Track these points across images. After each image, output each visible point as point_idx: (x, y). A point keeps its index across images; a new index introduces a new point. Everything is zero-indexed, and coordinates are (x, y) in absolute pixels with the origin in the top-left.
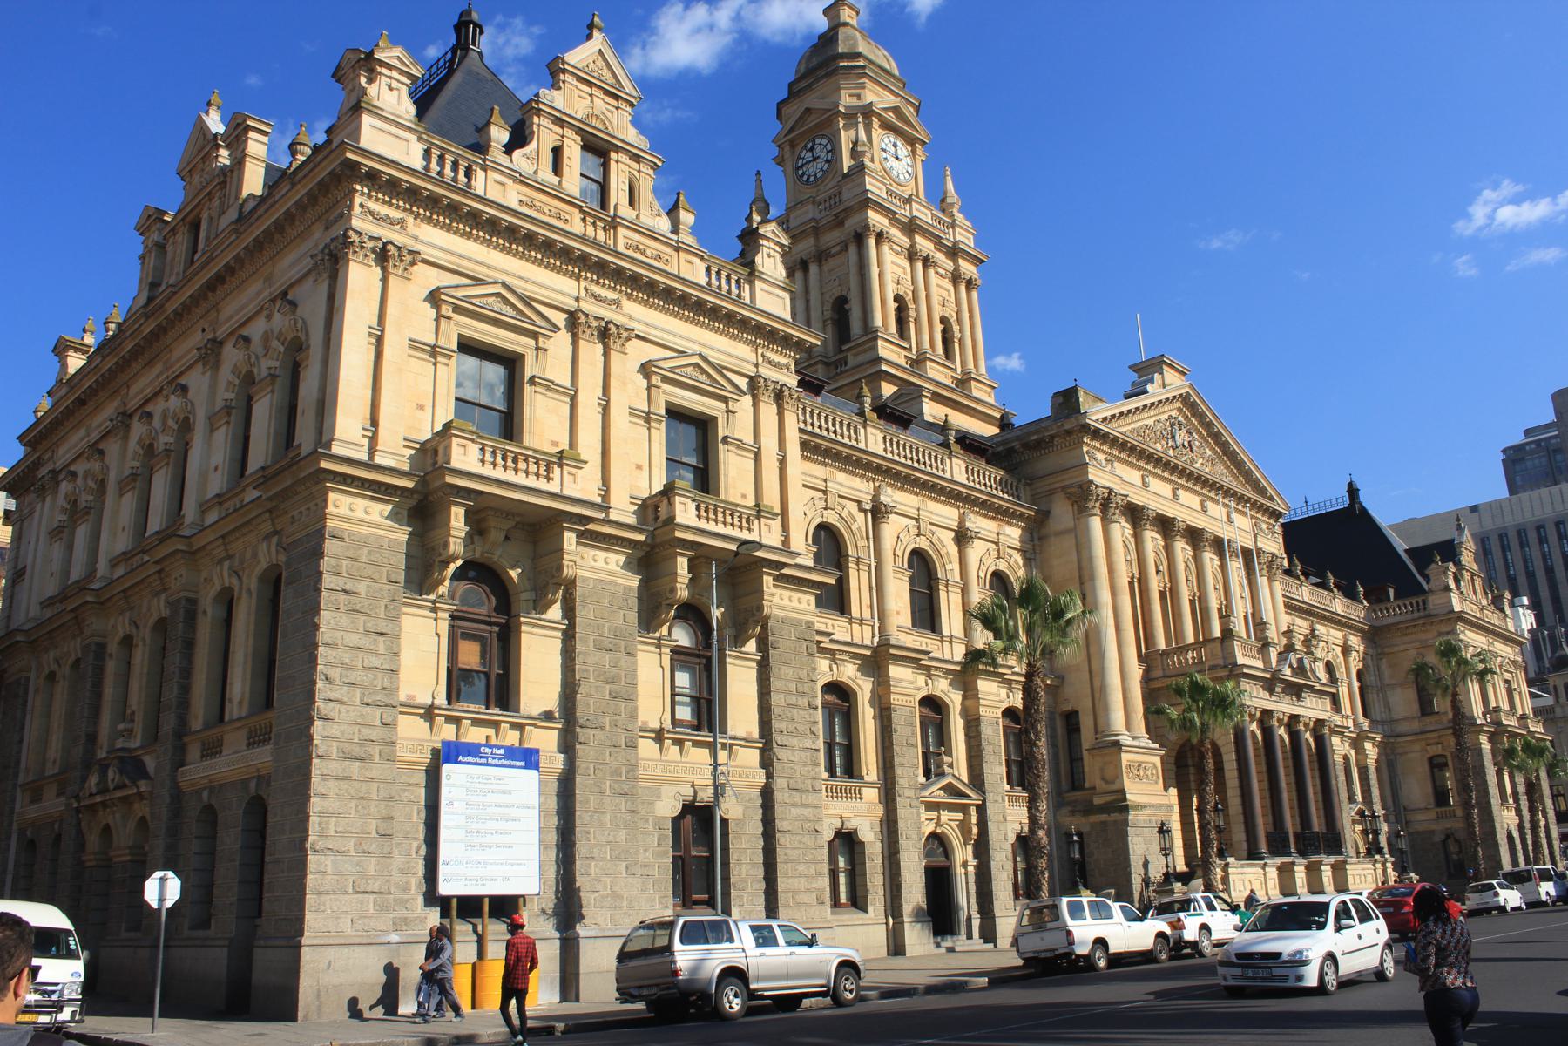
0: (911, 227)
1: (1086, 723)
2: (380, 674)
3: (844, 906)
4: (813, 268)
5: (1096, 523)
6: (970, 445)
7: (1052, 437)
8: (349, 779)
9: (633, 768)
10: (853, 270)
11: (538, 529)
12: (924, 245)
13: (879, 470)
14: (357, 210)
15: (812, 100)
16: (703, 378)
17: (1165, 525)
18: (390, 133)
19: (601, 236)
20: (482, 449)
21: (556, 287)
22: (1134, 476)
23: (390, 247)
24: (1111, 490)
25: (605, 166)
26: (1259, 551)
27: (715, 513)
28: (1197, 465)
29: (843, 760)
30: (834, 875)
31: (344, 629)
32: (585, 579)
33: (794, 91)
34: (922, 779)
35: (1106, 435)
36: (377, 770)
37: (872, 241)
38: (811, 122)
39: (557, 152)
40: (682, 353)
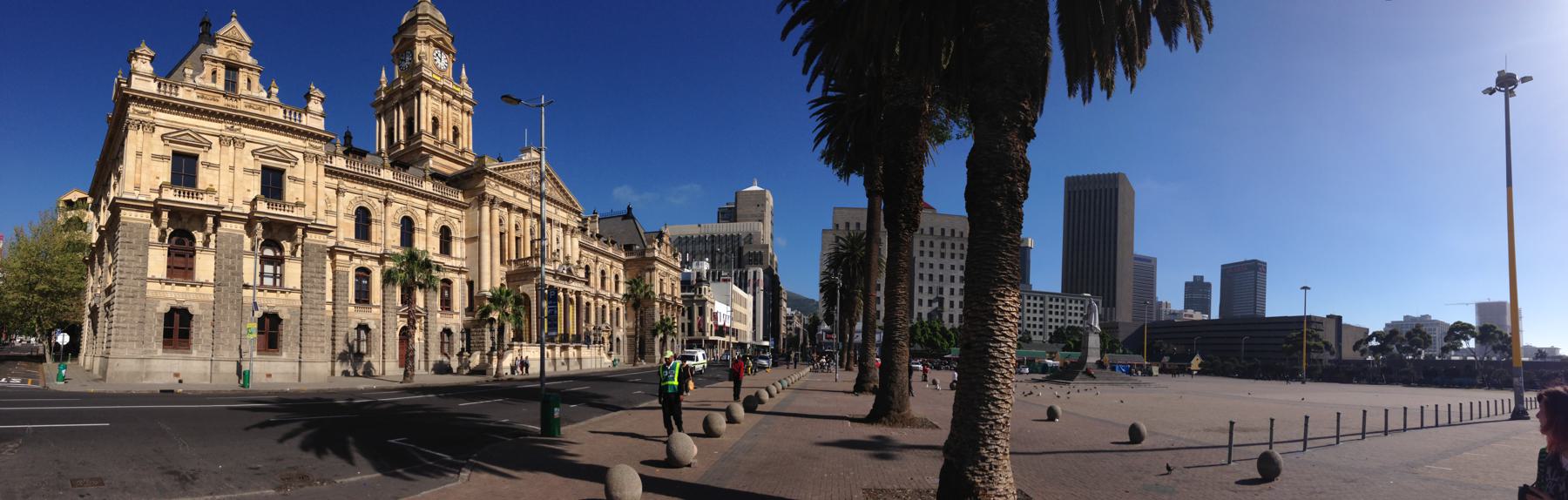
5: (486, 210)
6: (437, 176)
11: (198, 217)
15: (408, 34)
18: (144, 83)
22: (510, 192)
37: (423, 95)
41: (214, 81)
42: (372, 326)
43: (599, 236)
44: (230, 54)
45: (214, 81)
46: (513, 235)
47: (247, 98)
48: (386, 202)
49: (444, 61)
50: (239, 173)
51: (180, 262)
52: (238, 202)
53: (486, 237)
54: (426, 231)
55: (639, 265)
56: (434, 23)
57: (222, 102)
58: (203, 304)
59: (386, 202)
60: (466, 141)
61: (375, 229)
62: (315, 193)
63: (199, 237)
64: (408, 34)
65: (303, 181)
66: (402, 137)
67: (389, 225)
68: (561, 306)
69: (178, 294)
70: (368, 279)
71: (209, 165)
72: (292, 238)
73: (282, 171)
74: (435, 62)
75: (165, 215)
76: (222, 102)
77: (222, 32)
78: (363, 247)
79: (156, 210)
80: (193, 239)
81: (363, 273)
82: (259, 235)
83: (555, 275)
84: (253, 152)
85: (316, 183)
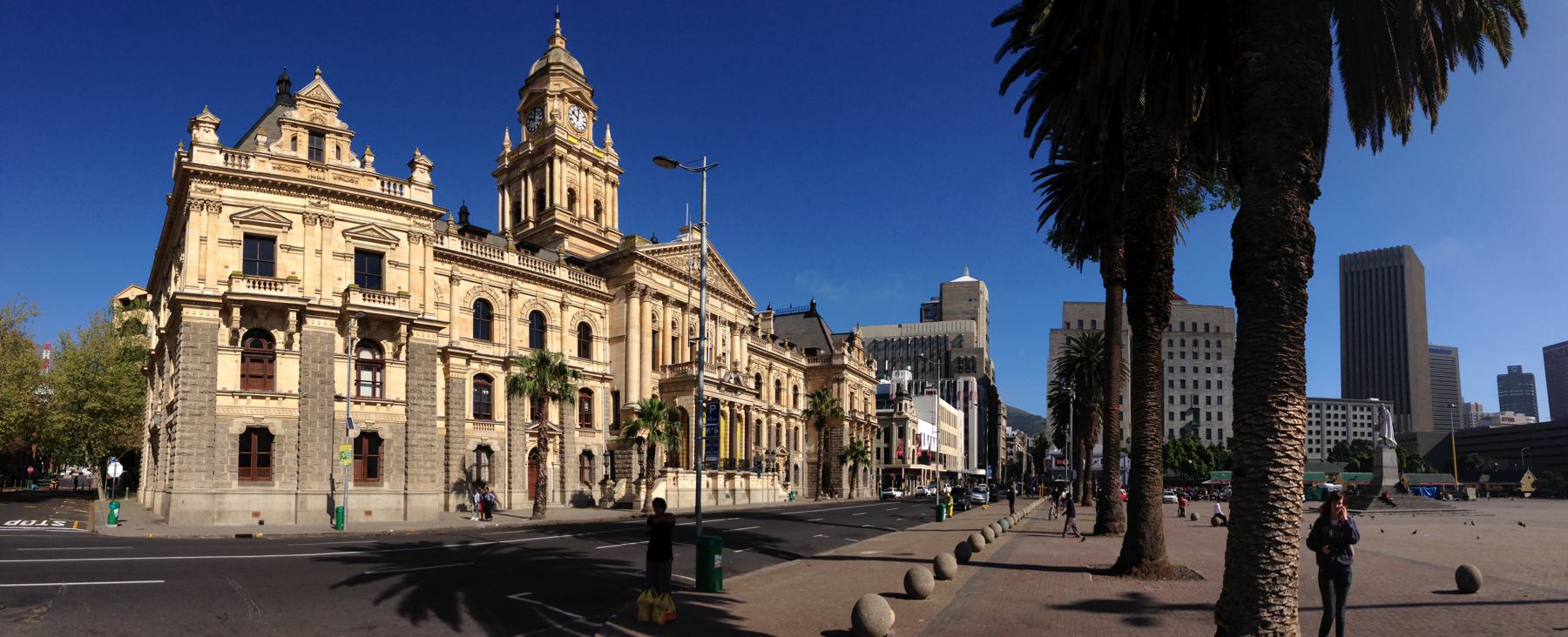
0: (581, 154)
11: (278, 312)
15: (536, 88)
37: (556, 162)
41: (295, 148)
42: (495, 447)
43: (774, 338)
44: (314, 117)
45: (295, 148)
46: (669, 333)
47: (336, 168)
48: (512, 293)
49: (582, 121)
50: (327, 255)
51: (256, 368)
52: (327, 293)
53: (634, 336)
54: (561, 329)
55: (824, 373)
56: (570, 74)
57: (305, 173)
58: (286, 421)
60: (611, 218)
61: (498, 327)
62: (421, 280)
63: (280, 336)
64: (536, 88)
65: (408, 266)
66: (531, 213)
67: (515, 321)
68: (724, 425)
70: (490, 388)
71: (289, 249)
72: (394, 337)
73: (381, 255)
74: (570, 121)
76: (305, 173)
77: (304, 92)
78: (483, 348)
79: (225, 307)
80: (272, 340)
81: (484, 381)
82: (354, 334)
83: (720, 385)
84: (344, 233)
85: (423, 269)
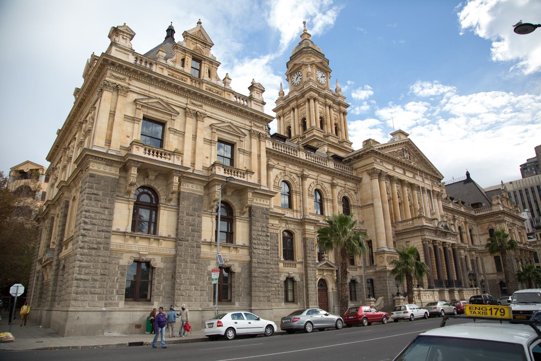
1: (374, 244)
2: (105, 221)
3: (290, 302)
4: (296, 110)
7: (363, 154)
8: (91, 255)
9: (199, 254)
10: (307, 110)
12: (330, 102)
13: (303, 163)
14: (108, 75)
15: (297, 61)
16: (231, 130)
17: (401, 182)
19: (197, 86)
20: (145, 149)
21: (178, 100)
22: (390, 167)
23: (119, 86)
24: (381, 170)
25: (200, 66)
26: (433, 191)
27: (231, 172)
28: (412, 164)
29: (289, 254)
30: (286, 292)
31: (93, 206)
32: (184, 192)
33: (292, 59)
34: (317, 261)
35: (380, 153)
36: (102, 252)
37: (312, 101)
38: (296, 67)
39: (183, 60)
40: (223, 122)
46: (397, 201)
59: (303, 177)
64: (297, 61)
69: (142, 247)
75: (134, 171)
